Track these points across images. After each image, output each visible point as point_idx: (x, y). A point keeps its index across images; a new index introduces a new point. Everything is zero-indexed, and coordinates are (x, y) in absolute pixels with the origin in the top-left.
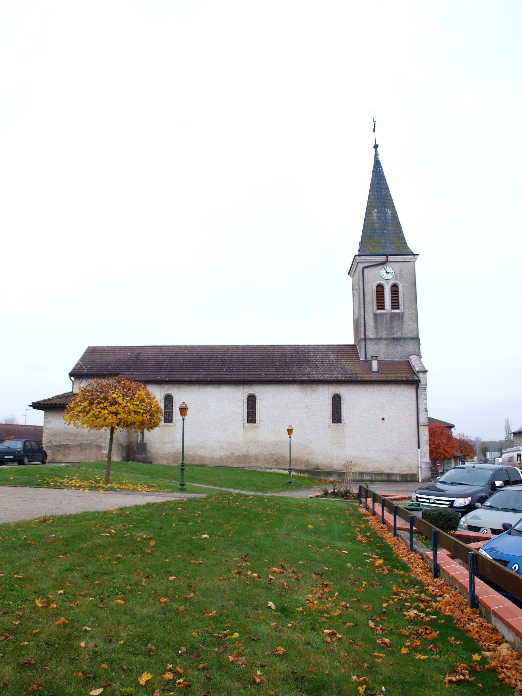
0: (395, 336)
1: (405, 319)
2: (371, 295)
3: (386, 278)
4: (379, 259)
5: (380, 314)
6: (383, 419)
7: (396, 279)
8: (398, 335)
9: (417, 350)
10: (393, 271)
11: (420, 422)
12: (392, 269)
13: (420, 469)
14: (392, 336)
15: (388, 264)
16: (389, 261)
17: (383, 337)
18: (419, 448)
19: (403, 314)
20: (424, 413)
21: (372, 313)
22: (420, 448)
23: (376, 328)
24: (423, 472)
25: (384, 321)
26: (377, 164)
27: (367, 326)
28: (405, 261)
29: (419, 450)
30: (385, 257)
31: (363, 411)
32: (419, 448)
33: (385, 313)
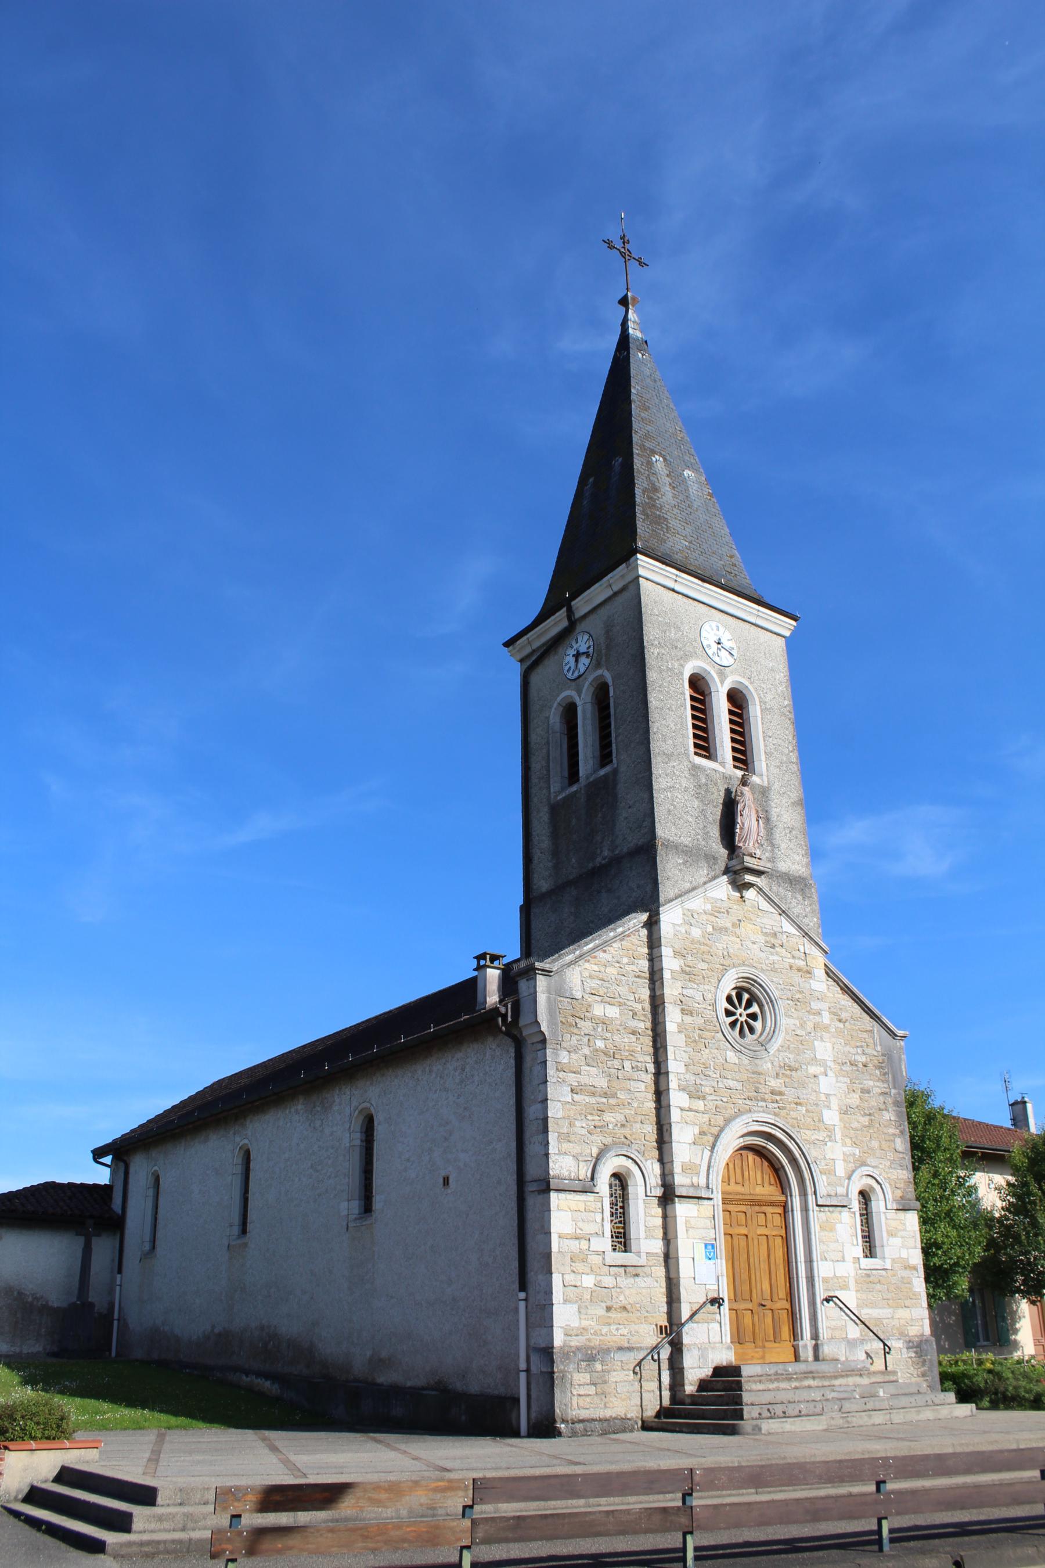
0: (599, 860)
1: (621, 788)
2: (545, 751)
3: (576, 674)
4: (555, 624)
5: (564, 798)
6: (446, 1181)
7: (598, 665)
8: (606, 853)
9: (649, 888)
10: (591, 643)
11: (528, 1178)
12: (586, 637)
13: (523, 1376)
14: (591, 865)
15: (580, 627)
16: (578, 614)
17: (571, 878)
18: (523, 1286)
19: (615, 772)
20: (541, 1137)
21: (546, 809)
22: (531, 1291)
23: (555, 853)
24: (534, 1395)
25: (574, 821)
26: (624, 341)
27: (537, 854)
28: (616, 594)
29: (522, 1295)
30: (563, 612)
31: (408, 1160)
32: (523, 1286)
33: (576, 792)
